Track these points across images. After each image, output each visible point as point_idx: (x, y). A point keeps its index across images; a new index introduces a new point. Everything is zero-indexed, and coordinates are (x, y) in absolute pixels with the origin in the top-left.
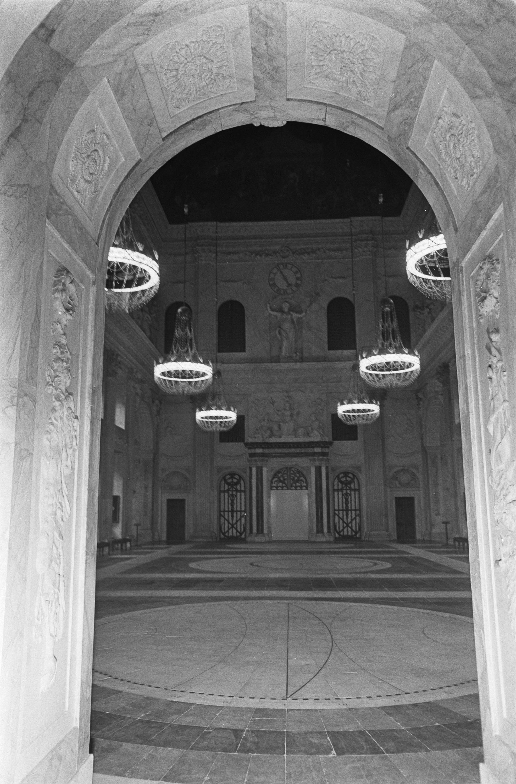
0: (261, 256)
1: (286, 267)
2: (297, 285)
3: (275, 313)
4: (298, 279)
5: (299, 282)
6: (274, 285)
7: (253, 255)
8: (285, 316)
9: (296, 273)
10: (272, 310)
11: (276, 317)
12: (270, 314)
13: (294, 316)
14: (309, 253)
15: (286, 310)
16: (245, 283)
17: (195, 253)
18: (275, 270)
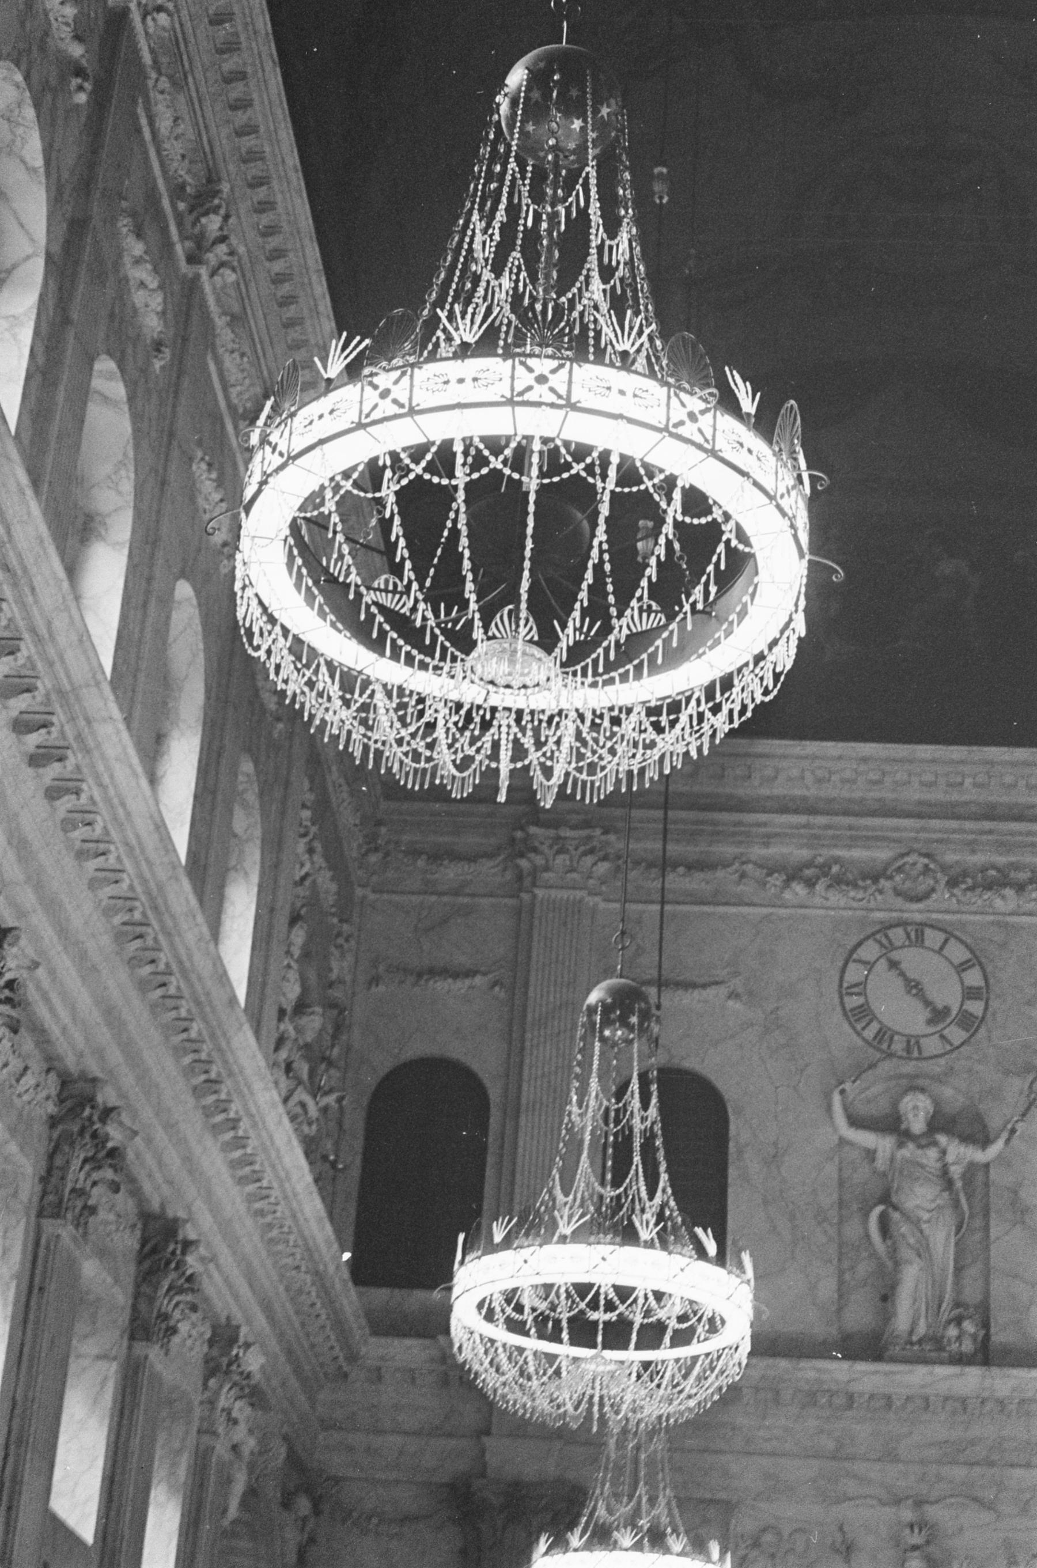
0: (810, 883)
1: (919, 940)
2: (966, 1021)
3: (866, 1139)
4: (970, 993)
5: (976, 1007)
6: (863, 1014)
7: (777, 880)
8: (909, 1151)
9: (962, 968)
10: (855, 1122)
11: (870, 1155)
12: (843, 1142)
13: (950, 1158)
14: (1020, 888)
15: (918, 1125)
16: (734, 995)
17: (522, 855)
18: (869, 951)
